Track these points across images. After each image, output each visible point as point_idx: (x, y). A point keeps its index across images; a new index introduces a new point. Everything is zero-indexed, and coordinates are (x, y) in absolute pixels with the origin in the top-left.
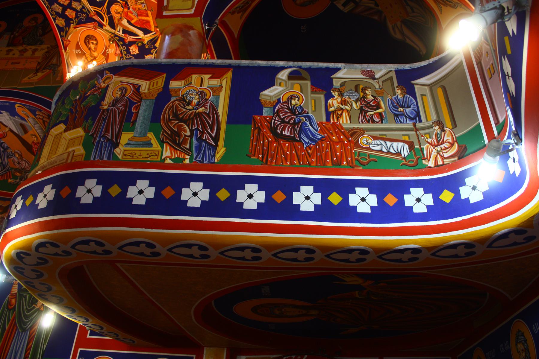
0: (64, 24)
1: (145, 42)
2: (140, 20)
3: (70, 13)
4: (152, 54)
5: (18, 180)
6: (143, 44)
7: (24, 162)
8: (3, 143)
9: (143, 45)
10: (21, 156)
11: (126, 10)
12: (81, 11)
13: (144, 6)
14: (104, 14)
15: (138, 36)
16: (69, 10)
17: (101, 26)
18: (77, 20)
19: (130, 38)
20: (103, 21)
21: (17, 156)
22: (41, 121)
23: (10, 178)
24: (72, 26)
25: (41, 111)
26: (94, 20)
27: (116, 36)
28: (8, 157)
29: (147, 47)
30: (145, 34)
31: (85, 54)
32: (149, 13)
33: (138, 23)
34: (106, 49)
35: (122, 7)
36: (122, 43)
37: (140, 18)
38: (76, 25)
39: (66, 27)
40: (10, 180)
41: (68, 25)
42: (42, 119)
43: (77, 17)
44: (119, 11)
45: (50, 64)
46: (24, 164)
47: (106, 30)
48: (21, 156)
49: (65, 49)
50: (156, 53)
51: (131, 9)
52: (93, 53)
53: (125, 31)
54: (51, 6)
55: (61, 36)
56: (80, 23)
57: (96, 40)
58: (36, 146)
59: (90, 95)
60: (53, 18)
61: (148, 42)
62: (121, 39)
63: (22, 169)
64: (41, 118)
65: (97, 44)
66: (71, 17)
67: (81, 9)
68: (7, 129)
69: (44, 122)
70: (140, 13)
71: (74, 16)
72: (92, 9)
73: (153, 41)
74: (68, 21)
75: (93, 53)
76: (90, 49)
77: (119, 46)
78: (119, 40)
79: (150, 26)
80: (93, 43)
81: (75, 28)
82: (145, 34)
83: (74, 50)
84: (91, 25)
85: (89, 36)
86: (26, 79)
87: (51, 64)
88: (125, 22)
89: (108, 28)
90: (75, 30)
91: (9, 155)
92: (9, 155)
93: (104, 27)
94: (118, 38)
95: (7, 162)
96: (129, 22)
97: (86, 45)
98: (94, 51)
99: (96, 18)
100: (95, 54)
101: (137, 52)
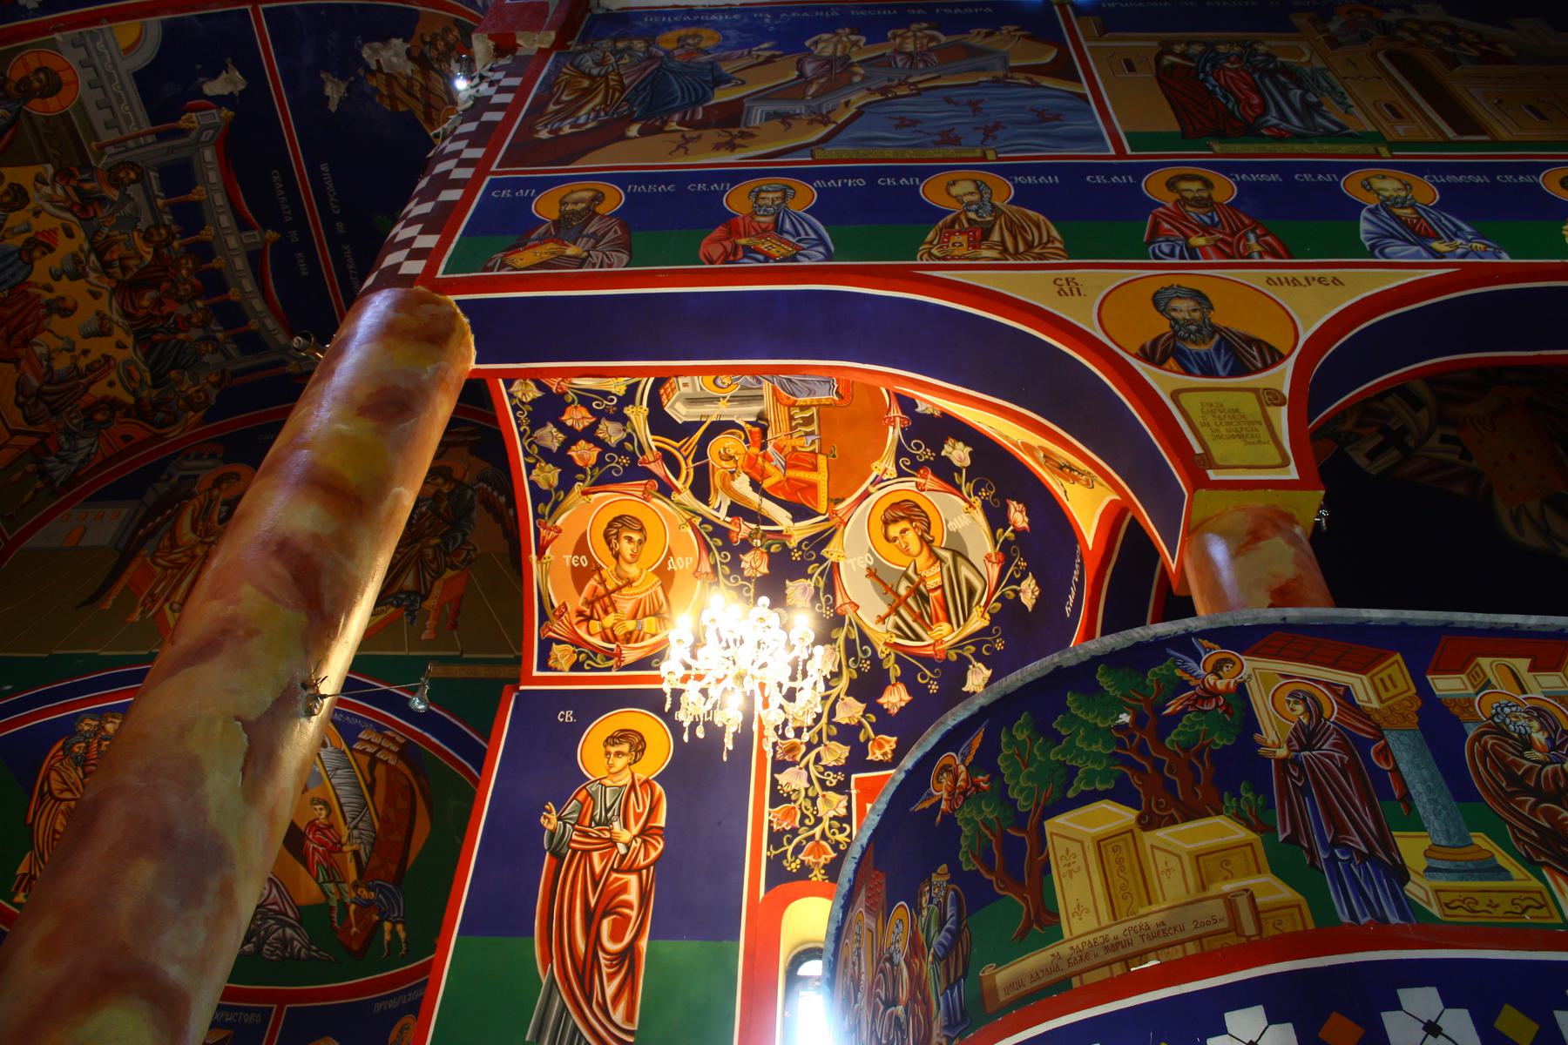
0: (555, 482)
1: (793, 543)
2: (788, 480)
3: (584, 453)
4: (810, 577)
6: (784, 546)
9: (786, 550)
11: (755, 450)
12: (620, 449)
13: (813, 443)
14: (686, 458)
15: (774, 524)
16: (582, 443)
17: (666, 490)
18: (597, 472)
19: (744, 529)
20: (677, 477)
22: (364, 760)
24: (578, 487)
25: (380, 729)
26: (650, 475)
27: (705, 520)
29: (796, 556)
30: (795, 520)
31: (599, 569)
32: (822, 461)
33: (783, 489)
34: (667, 558)
35: (746, 441)
36: (720, 543)
37: (791, 473)
38: (593, 485)
39: (557, 490)
41: (566, 484)
42: (373, 755)
43: (600, 461)
44: (732, 452)
45: (396, 589)
47: (679, 504)
49: (541, 553)
50: (821, 574)
51: (770, 449)
52: (626, 567)
53: (736, 510)
54: (533, 431)
55: (537, 516)
56: (604, 480)
57: (642, 530)
58: (318, 835)
59: (1184, 711)
60: (527, 464)
61: (800, 543)
62: (720, 532)
64: (370, 749)
65: (640, 542)
66: (580, 464)
67: (621, 444)
69: (374, 761)
70: (795, 460)
71: (593, 461)
72: (653, 444)
73: (819, 541)
74: (570, 473)
75: (626, 567)
76: (617, 556)
77: (709, 550)
78: (711, 535)
79: (815, 498)
80: (630, 539)
81: (585, 493)
82: (795, 520)
83: (567, 557)
84: (636, 488)
85: (621, 517)
87: (401, 591)
88: (742, 484)
89: (687, 497)
90: (583, 500)
93: (675, 496)
94: (710, 528)
96: (755, 486)
97: (609, 543)
98: (630, 563)
99: (660, 469)
100: (632, 571)
101: (764, 569)
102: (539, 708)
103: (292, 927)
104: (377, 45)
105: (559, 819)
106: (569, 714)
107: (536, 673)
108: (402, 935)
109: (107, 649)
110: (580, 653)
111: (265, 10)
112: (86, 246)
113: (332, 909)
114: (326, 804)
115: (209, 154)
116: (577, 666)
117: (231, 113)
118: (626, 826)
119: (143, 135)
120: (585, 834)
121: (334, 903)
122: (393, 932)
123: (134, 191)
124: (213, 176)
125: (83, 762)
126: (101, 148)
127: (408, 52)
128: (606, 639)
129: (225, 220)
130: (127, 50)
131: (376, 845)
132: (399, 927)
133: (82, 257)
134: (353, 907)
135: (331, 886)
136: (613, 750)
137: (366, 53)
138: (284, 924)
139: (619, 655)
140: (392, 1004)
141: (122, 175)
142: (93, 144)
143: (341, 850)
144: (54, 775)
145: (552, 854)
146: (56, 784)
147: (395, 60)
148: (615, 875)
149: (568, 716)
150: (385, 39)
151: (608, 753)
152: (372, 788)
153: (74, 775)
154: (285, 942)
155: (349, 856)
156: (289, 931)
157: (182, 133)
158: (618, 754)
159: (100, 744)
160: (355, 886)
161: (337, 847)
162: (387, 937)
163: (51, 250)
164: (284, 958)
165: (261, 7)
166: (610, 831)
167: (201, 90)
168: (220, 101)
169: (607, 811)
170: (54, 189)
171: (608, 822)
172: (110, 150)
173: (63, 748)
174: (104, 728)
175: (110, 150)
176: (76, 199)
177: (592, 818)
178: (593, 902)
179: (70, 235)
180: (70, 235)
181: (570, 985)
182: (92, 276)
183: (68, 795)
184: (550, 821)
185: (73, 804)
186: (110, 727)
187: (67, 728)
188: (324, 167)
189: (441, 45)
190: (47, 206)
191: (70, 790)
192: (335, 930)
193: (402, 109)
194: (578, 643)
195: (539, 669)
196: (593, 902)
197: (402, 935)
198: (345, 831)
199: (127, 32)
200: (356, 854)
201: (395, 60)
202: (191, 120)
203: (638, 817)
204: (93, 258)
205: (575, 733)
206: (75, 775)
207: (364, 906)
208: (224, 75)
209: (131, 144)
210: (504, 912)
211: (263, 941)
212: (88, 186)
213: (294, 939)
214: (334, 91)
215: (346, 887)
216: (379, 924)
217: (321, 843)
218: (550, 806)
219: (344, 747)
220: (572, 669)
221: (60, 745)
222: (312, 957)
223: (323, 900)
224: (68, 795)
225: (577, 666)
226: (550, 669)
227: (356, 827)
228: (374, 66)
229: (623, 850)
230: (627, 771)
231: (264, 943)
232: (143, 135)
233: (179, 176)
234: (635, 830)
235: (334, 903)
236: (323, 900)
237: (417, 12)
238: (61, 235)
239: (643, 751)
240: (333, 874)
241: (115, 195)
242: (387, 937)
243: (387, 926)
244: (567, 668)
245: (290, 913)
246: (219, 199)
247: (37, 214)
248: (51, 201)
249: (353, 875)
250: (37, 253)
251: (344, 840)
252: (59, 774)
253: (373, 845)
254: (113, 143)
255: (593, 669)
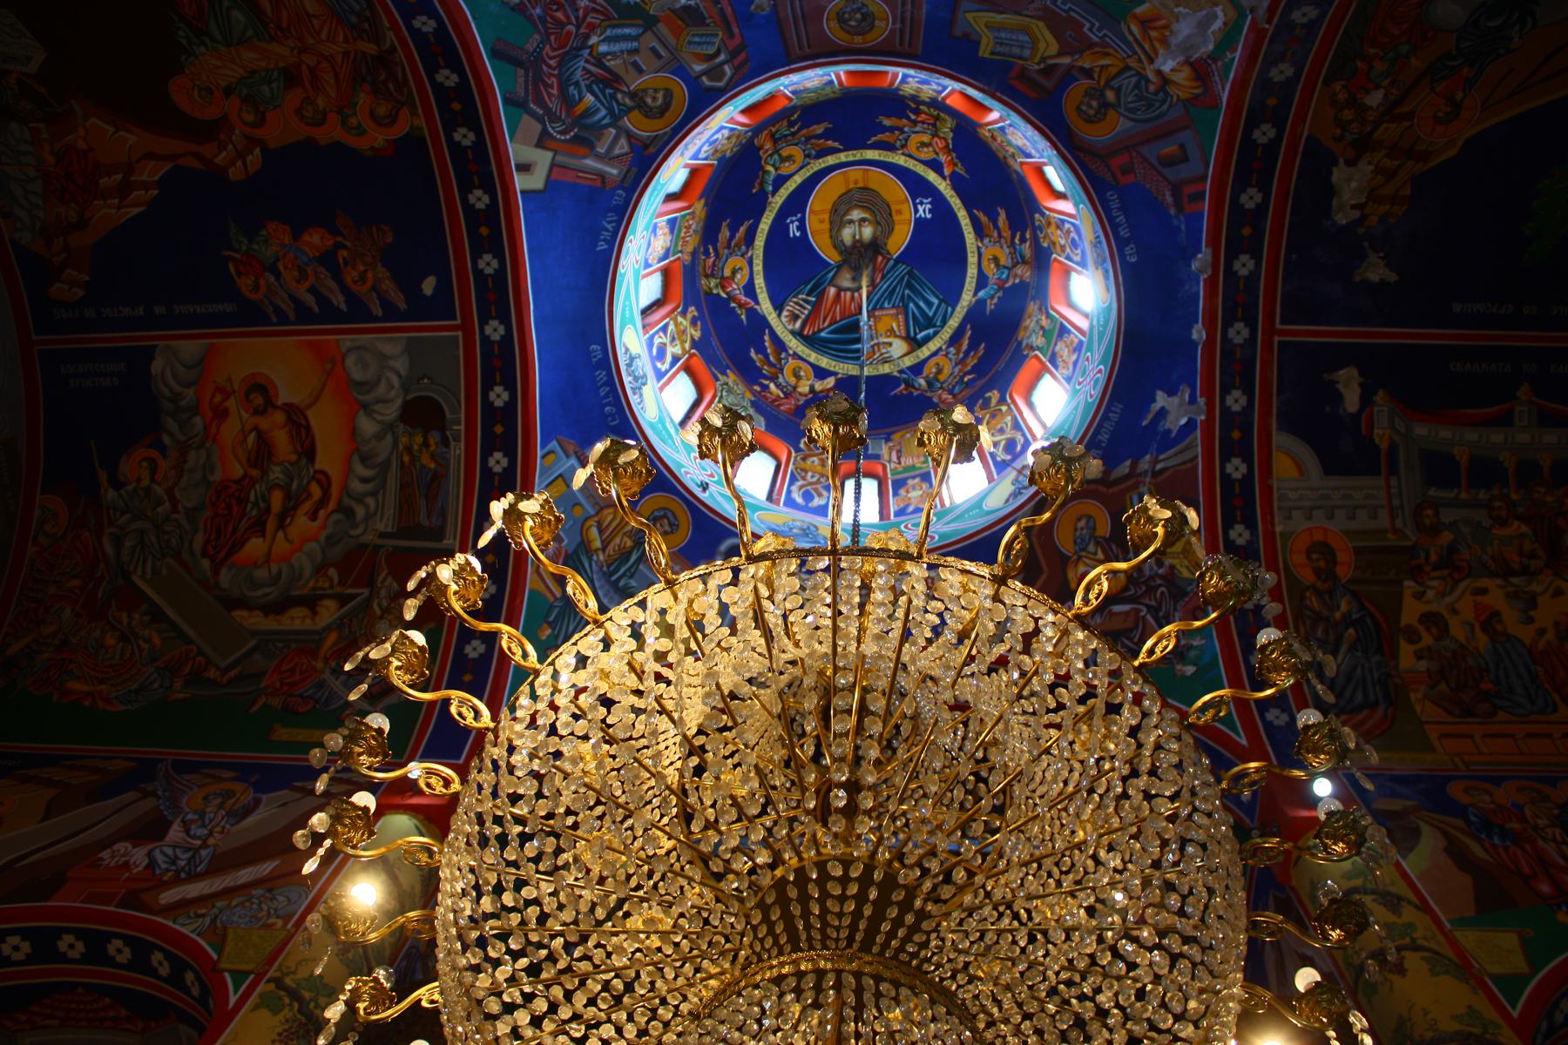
104: (1335, 202)
111: (1282, 323)
112: (1499, 581)
115: (1420, 430)
117: (1381, 393)
119: (1389, 487)
123: (1447, 516)
124: (1445, 433)
126: (1395, 531)
127: (1349, 163)
129: (1497, 437)
130: (1301, 473)
133: (1511, 589)
137: (1341, 219)
141: (1427, 522)
142: (1390, 536)
147: (1354, 185)
150: (1331, 191)
157: (1393, 449)
163: (1497, 614)
165: (1278, 326)
167: (1352, 415)
168: (1366, 401)
170: (1431, 588)
172: (1399, 523)
175: (1399, 523)
176: (1445, 572)
179: (1484, 591)
180: (1484, 591)
182: (1534, 587)
188: (1457, 308)
189: (1347, 114)
190: (1448, 600)
193: (1407, 191)
199: (1283, 467)
201: (1354, 185)
202: (1381, 434)
204: (1515, 580)
208: (1340, 386)
209: (1396, 502)
212: (1433, 557)
214: (1375, 271)
228: (1356, 214)
232: (1389, 487)
233: (1438, 468)
237: (1309, 138)
238: (1480, 599)
241: (1447, 537)
246: (1472, 435)
247: (1455, 612)
248: (1443, 595)
250: (1499, 627)
254: (1392, 518)
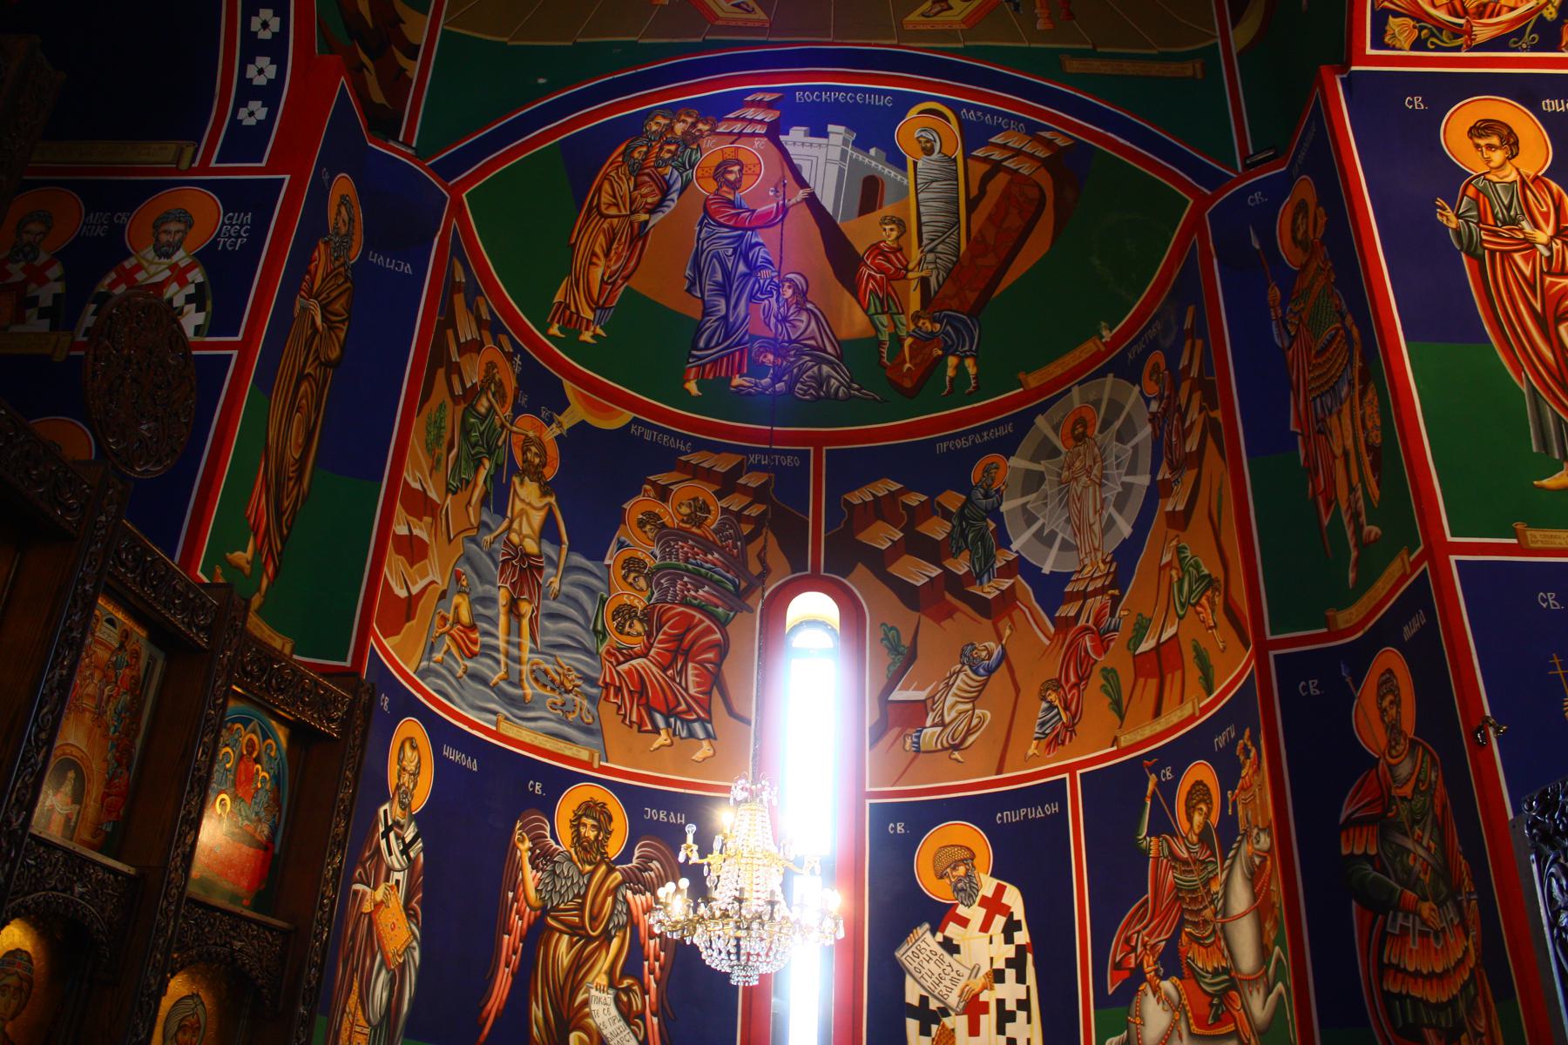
5: (767, 380)
7: (804, 317)
8: (758, 244)
10: (805, 294)
21: (788, 293)
22: (978, 170)
23: (739, 371)
28: (752, 297)
40: (737, 381)
46: (803, 326)
48: (801, 295)
58: (880, 260)
63: (791, 341)
68: (802, 194)
86: (914, 17)
91: (761, 290)
92: (761, 290)
95: (742, 314)
102: (1378, 95)
103: (829, 363)
105: (1458, 216)
106: (1418, 100)
107: (1369, 51)
108: (972, 370)
109: (644, 36)
110: (1421, 29)
113: (881, 343)
114: (901, 224)
116: (1418, 45)
118: (1537, 226)
120: (1495, 234)
121: (885, 337)
122: (960, 367)
125: (637, 171)
128: (1453, 12)
131: (955, 272)
132: (969, 363)
134: (909, 341)
135: (884, 319)
136: (1482, 142)
138: (820, 361)
139: (1470, 33)
140: (961, 444)
143: (904, 277)
144: (606, 186)
145: (1467, 254)
146: (605, 198)
148: (1548, 279)
149: (1417, 103)
151: (1478, 146)
152: (972, 205)
153: (625, 187)
154: (820, 381)
155: (914, 283)
156: (826, 369)
158: (1490, 147)
159: (661, 148)
160: (916, 317)
161: (901, 274)
162: (950, 372)
164: (819, 398)
166: (1521, 230)
169: (1509, 208)
171: (1514, 221)
173: (623, 153)
174: (672, 129)
177: (1495, 217)
178: (1538, 307)
181: (1550, 388)
183: (613, 211)
184: (1449, 219)
185: (615, 221)
186: (679, 128)
187: (634, 128)
191: (617, 205)
192: (883, 366)
194: (1419, 16)
195: (1373, 47)
196: (1538, 307)
197: (972, 370)
198: (915, 254)
200: (924, 282)
203: (1546, 216)
205: (1432, 120)
206: (626, 187)
207: (923, 340)
210: (1445, 314)
211: (795, 380)
213: (829, 377)
215: (903, 318)
216: (940, 361)
217: (880, 269)
218: (1440, 202)
219: (959, 154)
220: (1413, 48)
221: (623, 148)
222: (849, 397)
223: (872, 332)
224: (613, 211)
225: (1418, 45)
226: (1387, 47)
227: (931, 251)
229: (1546, 253)
230: (1509, 167)
231: (797, 381)
234: (1550, 231)
235: (885, 337)
236: (872, 332)
239: (1516, 143)
240: (889, 303)
242: (950, 372)
243: (952, 361)
244: (1407, 46)
245: (829, 349)
249: (915, 303)
251: (911, 266)
252: (614, 186)
253: (949, 272)
255: (1438, 49)
